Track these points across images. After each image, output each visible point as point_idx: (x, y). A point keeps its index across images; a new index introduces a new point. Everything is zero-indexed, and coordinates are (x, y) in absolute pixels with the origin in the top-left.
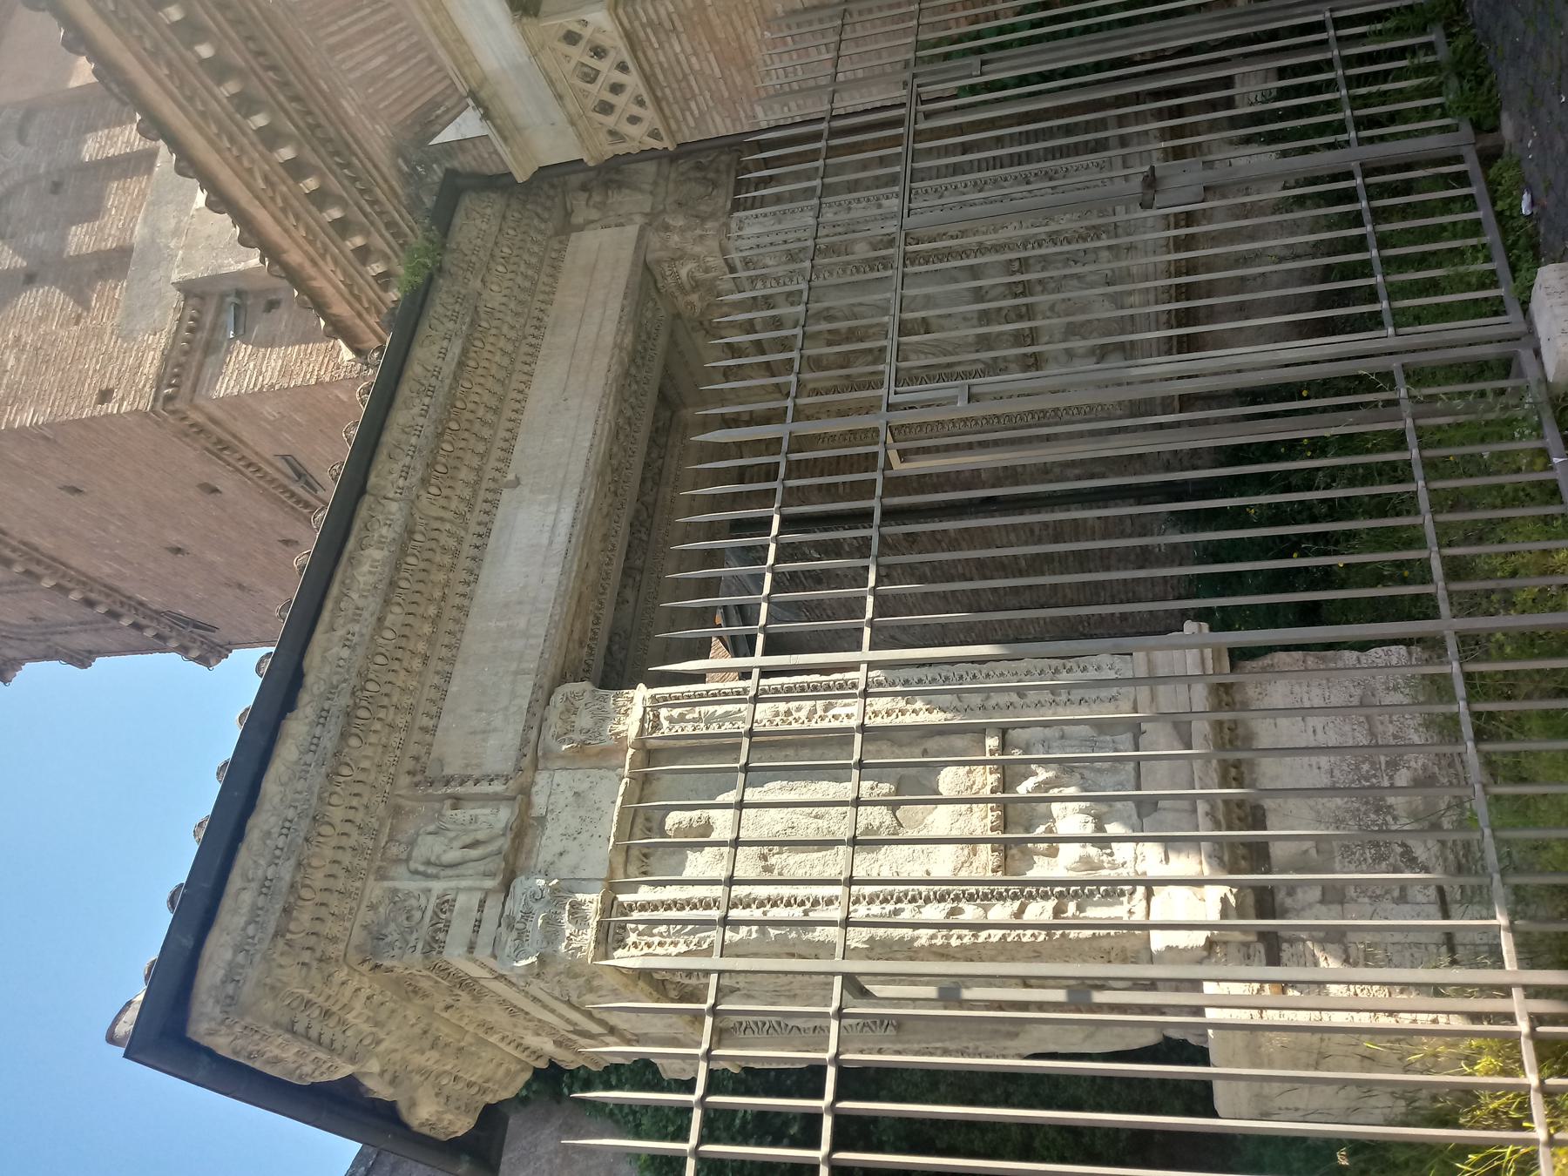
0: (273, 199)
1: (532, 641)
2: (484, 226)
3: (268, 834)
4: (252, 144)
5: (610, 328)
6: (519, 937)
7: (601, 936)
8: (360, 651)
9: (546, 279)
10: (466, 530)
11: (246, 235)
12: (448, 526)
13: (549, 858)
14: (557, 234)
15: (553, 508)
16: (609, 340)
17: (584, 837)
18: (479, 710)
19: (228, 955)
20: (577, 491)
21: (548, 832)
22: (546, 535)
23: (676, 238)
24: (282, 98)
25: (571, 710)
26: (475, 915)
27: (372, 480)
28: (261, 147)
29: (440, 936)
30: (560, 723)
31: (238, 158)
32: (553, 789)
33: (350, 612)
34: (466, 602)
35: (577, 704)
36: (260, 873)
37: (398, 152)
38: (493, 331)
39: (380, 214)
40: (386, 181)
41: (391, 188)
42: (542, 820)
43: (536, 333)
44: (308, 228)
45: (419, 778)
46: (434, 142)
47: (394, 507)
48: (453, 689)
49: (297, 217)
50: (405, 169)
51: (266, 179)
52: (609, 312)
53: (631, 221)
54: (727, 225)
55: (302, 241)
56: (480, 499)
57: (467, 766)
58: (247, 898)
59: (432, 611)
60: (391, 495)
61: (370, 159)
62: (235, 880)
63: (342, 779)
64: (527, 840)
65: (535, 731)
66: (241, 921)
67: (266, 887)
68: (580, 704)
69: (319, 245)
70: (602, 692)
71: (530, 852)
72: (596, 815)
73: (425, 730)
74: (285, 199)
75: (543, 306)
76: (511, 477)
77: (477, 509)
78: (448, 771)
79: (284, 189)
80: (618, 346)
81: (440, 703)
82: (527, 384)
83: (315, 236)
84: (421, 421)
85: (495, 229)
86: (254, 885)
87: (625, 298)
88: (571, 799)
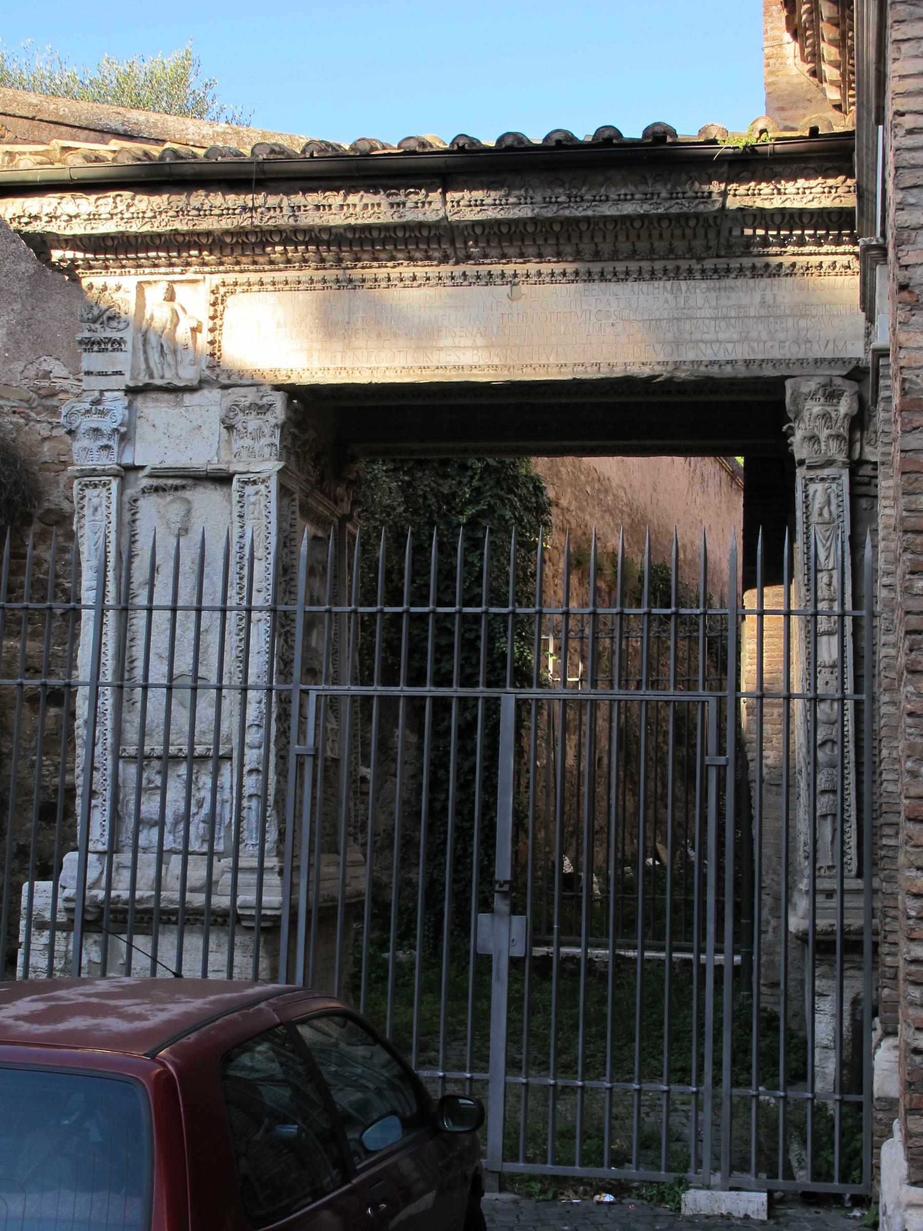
5: (708, 354)
6: (88, 412)
10: (457, 263)
13: (151, 417)
16: (691, 356)
17: (165, 441)
21: (171, 411)
23: (817, 410)
25: (263, 409)
26: (110, 370)
29: (96, 348)
30: (247, 403)
33: (324, 202)
35: (269, 413)
38: (689, 232)
42: (178, 404)
47: (437, 205)
52: (730, 346)
54: (829, 463)
64: (166, 396)
68: (269, 417)
70: (278, 432)
71: (157, 400)
72: (182, 447)
80: (677, 365)
82: (640, 278)
87: (747, 363)
88: (195, 423)
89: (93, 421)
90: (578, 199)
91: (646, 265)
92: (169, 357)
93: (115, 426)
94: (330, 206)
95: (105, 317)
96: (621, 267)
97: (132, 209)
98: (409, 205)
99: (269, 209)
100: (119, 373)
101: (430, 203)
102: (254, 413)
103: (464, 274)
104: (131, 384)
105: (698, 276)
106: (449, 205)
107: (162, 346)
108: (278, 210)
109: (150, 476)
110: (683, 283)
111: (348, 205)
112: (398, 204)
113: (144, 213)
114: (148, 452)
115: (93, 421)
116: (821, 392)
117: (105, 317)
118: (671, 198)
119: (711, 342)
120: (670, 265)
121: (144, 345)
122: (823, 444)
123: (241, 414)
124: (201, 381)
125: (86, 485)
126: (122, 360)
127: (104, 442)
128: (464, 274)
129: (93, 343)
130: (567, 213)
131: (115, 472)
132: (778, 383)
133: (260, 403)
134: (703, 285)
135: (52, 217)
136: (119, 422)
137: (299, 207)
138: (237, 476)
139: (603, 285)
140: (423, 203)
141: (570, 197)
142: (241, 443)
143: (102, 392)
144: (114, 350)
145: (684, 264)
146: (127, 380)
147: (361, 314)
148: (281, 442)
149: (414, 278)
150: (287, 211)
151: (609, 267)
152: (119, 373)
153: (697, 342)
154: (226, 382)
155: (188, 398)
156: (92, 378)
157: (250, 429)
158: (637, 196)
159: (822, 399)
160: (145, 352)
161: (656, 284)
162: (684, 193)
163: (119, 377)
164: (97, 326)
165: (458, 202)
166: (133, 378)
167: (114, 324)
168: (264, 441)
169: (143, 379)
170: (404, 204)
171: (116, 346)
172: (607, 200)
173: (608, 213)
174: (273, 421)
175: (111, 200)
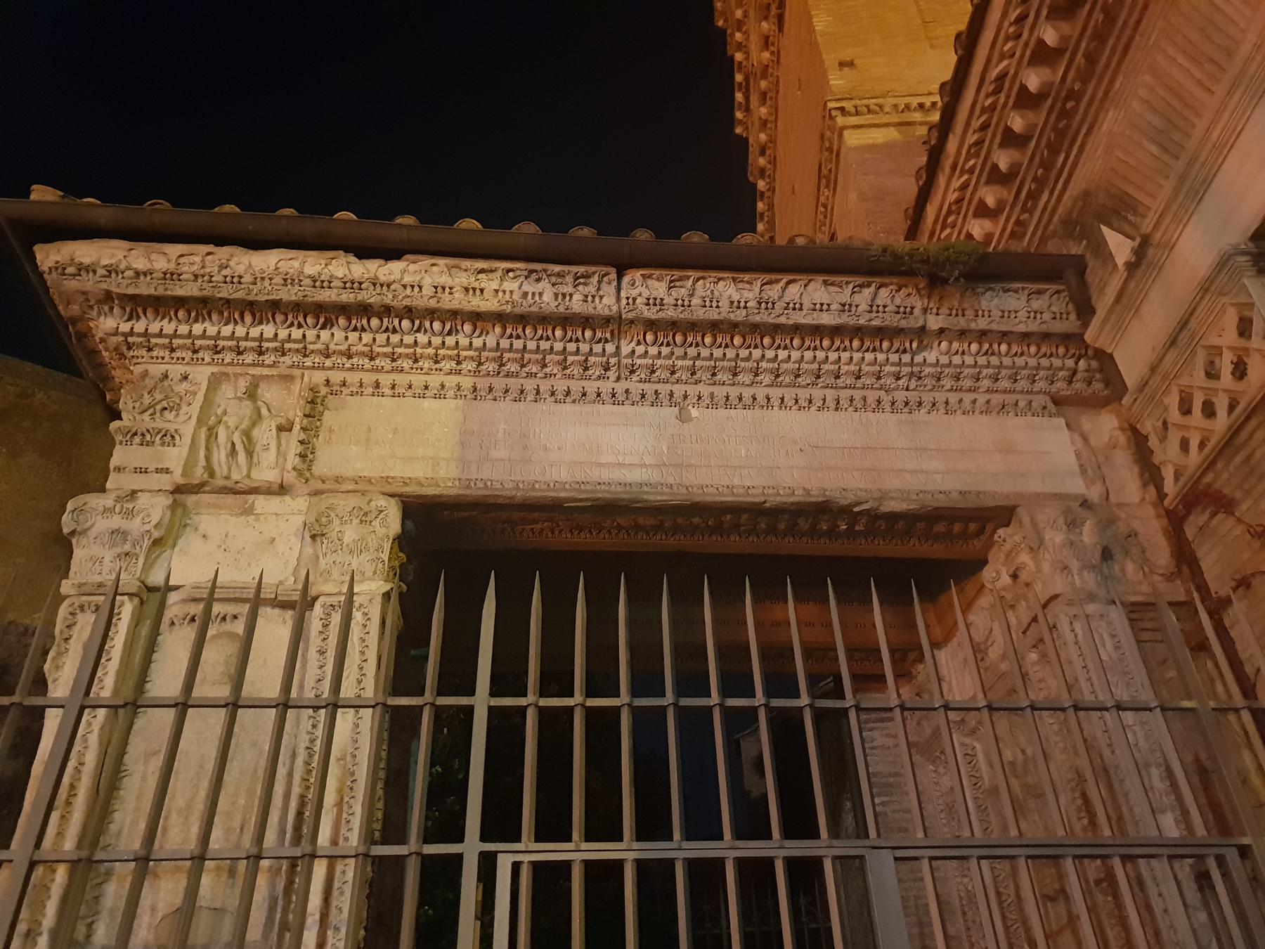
0: (987, 96)
1: (474, 467)
2: (1022, 315)
3: (222, 267)
4: (1026, 44)
7: (87, 589)
8: (433, 303)
9: (982, 399)
11: (948, 88)
12: (613, 361)
13: (202, 527)
14: (1056, 402)
15: (648, 460)
18: (395, 431)
19: (105, 262)
20: (670, 480)
21: (233, 519)
22: (611, 459)
24: (1083, 45)
27: (637, 274)
28: (1028, 53)
29: (137, 439)
31: (1008, 38)
32: (287, 516)
33: (476, 285)
34: (530, 397)
35: (376, 523)
36: (185, 269)
37: (1086, 195)
39: (1024, 209)
40: (1059, 200)
41: (1054, 210)
42: (248, 511)
43: (900, 405)
44: (979, 143)
45: (324, 390)
46: (1104, 229)
47: (609, 300)
48: (427, 404)
49: (984, 127)
50: (1075, 214)
51: (1002, 77)
53: (1089, 482)
55: (966, 147)
56: (659, 387)
57: (331, 431)
58: (160, 264)
59: (513, 367)
60: (623, 294)
61: (1070, 175)
62: (175, 250)
63: (301, 319)
65: (350, 488)
66: (140, 264)
67: (171, 276)
69: (972, 162)
73: (377, 385)
74: (993, 108)
75: (942, 407)
76: (694, 412)
77: (646, 386)
78: (328, 417)
79: (1002, 100)
80: (884, 495)
81: (410, 393)
83: (977, 155)
84: (724, 304)
85: (1022, 328)
86: (172, 266)
89: (116, 522)
90: (770, 305)
91: (830, 394)
92: (242, 456)
93: (147, 527)
94: (482, 291)
95: (158, 407)
96: (803, 394)
97: (224, 272)
98: (577, 297)
99: (405, 287)
100: (167, 471)
101: (601, 297)
102: (356, 521)
103: (627, 391)
104: (181, 481)
105: (888, 408)
106: (624, 302)
107: (233, 444)
108: (416, 289)
109: (184, 601)
110: (870, 414)
111: (504, 292)
112: (564, 295)
113: (240, 277)
114: (187, 567)
115: (116, 522)
116: (1061, 520)
117: (158, 407)
118: (870, 312)
119: (916, 472)
120: (857, 395)
121: (208, 441)
122: (1076, 577)
123: (336, 522)
124: (282, 486)
125: (82, 607)
126: (175, 457)
127: (127, 547)
128: (627, 391)
129: (135, 434)
130: (757, 318)
131: (134, 590)
132: (1004, 514)
133: (366, 509)
134: (895, 417)
135: (111, 271)
136: (154, 522)
137: (444, 288)
138: (321, 599)
139: (783, 413)
140: (593, 297)
141: (760, 303)
142: (330, 558)
143: (134, 492)
144: (163, 444)
145: (872, 396)
146: (178, 477)
147: (502, 426)
148: (390, 559)
149: (568, 393)
150: (428, 291)
151: (789, 394)
152: (167, 471)
153: (900, 470)
154: (320, 486)
155: (262, 503)
156: (121, 476)
157: (346, 540)
158: (833, 307)
159: (1064, 528)
160: (207, 449)
161: (842, 414)
162: (885, 307)
163: (165, 476)
164: (146, 416)
165: (634, 299)
166: (184, 474)
167: (169, 415)
168: (365, 557)
169: (199, 474)
170: (571, 295)
171: (168, 439)
172: (801, 309)
173: (804, 321)
174: (381, 531)
175: (198, 259)
